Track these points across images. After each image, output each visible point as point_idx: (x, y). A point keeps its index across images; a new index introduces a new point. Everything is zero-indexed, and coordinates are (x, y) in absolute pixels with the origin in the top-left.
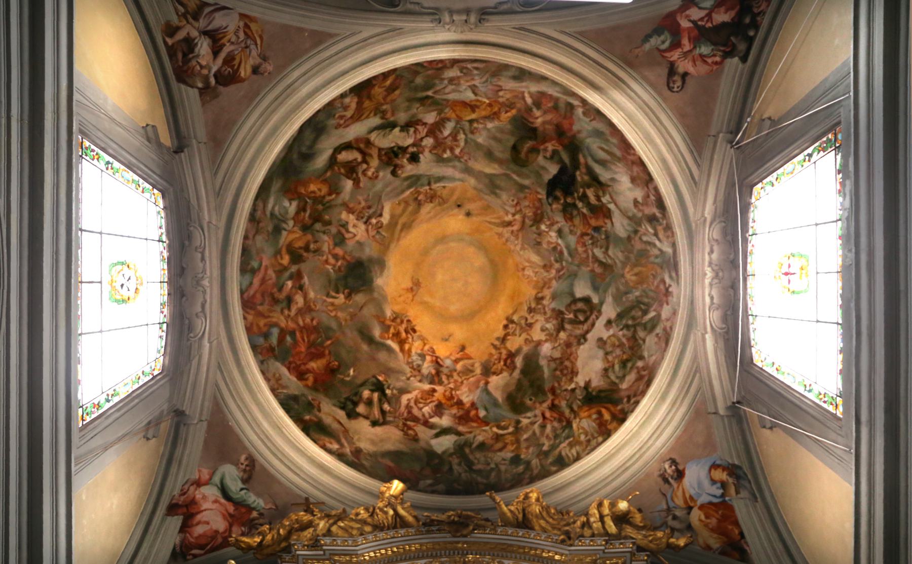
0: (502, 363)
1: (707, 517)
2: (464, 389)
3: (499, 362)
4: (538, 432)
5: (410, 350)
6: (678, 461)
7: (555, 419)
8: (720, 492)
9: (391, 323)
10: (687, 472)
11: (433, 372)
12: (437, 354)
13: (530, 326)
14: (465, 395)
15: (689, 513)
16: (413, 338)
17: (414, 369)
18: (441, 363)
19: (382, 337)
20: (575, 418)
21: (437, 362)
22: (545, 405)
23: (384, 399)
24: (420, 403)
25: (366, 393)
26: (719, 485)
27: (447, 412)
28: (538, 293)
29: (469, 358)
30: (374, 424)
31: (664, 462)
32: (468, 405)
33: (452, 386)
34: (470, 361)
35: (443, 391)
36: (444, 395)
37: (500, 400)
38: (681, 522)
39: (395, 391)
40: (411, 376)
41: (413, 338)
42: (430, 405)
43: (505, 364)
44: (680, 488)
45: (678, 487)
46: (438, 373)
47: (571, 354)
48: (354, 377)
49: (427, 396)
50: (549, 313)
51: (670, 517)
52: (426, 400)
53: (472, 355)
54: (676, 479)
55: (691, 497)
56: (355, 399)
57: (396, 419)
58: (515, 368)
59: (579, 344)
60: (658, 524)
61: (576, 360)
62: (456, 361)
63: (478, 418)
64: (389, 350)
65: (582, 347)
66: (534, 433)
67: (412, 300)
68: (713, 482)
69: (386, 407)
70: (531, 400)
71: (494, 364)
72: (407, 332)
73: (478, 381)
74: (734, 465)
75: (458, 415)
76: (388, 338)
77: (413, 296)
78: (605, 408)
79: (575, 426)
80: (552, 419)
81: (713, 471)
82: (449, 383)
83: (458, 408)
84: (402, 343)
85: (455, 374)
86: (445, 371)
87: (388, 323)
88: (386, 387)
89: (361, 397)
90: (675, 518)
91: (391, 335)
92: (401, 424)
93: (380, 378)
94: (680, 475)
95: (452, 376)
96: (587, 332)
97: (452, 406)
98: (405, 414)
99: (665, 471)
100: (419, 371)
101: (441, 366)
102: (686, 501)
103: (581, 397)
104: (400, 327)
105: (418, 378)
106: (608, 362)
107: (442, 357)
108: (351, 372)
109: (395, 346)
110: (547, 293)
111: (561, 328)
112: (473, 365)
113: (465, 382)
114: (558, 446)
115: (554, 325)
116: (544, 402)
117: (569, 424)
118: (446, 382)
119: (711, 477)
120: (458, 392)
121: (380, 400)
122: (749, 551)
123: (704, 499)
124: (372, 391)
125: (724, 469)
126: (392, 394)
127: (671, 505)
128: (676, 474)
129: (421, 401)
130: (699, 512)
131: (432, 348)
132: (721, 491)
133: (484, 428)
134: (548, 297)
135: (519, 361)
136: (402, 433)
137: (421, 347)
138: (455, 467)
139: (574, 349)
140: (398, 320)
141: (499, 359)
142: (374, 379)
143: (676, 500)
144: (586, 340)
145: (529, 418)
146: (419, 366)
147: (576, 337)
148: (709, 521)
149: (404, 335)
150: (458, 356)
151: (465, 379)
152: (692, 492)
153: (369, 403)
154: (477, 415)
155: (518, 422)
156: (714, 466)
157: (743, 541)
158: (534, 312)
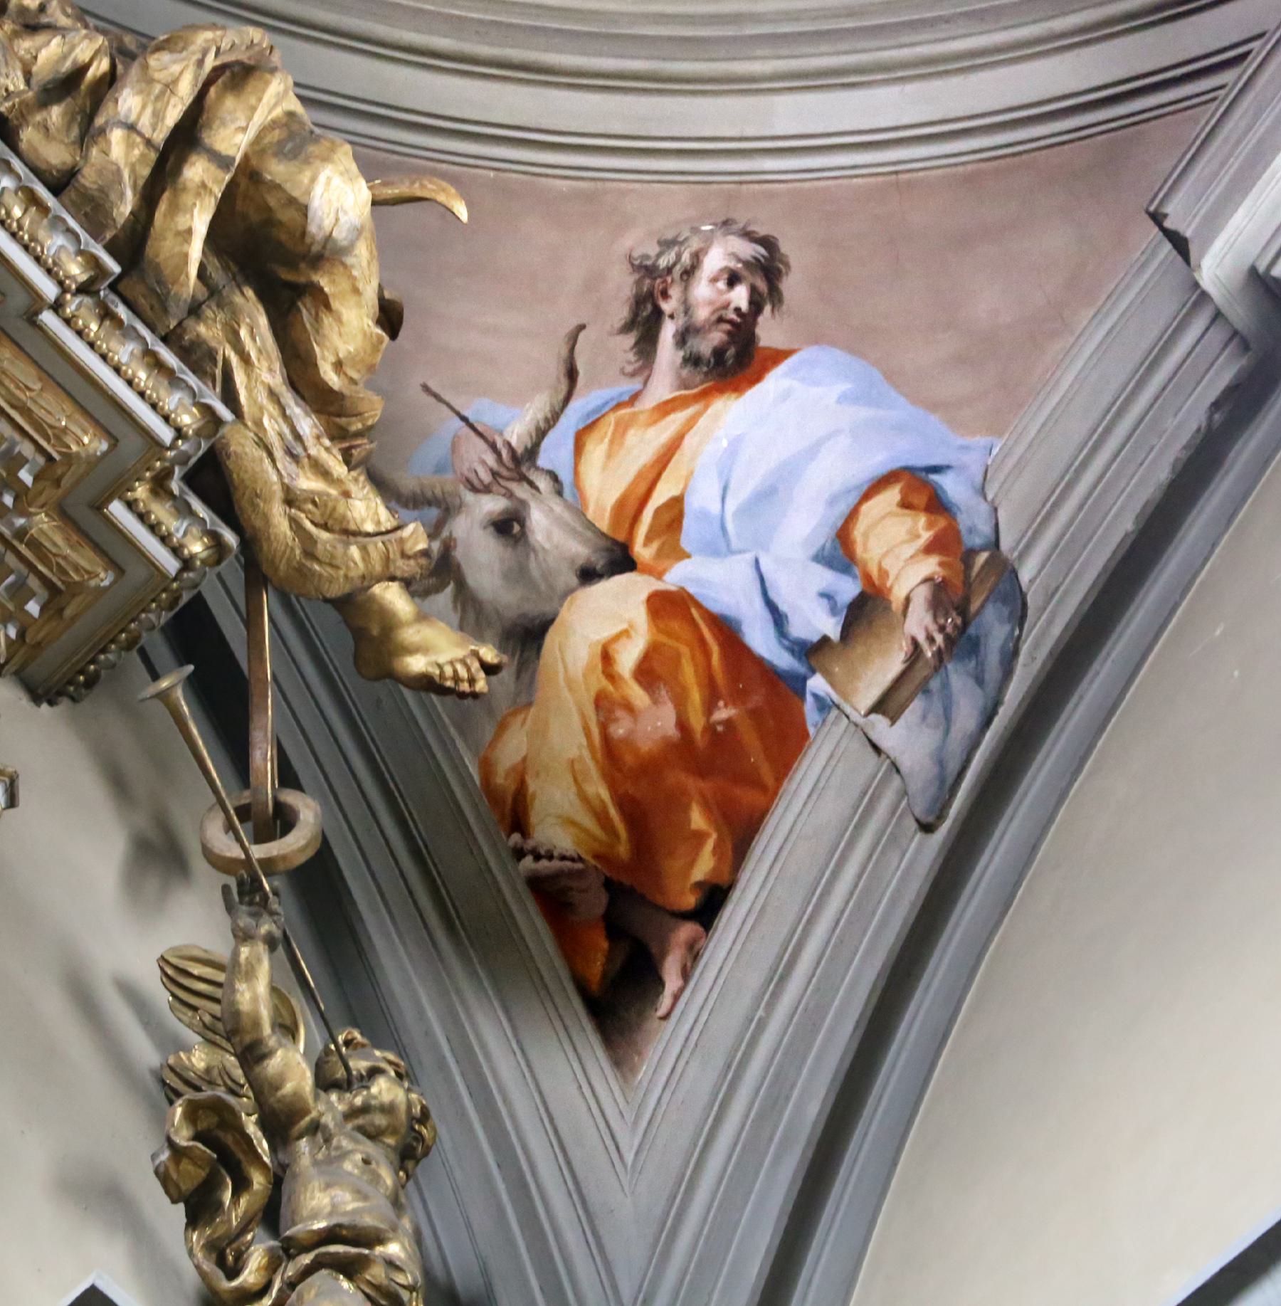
1: (647, 673)
6: (789, 285)
10: (775, 381)
15: (588, 575)
26: (848, 589)
31: (726, 224)
38: (518, 574)
44: (677, 419)
45: (666, 408)
51: (492, 505)
54: (693, 360)
55: (674, 514)
60: (408, 481)
74: (1004, 570)
81: (892, 495)
99: (689, 273)
102: (631, 508)
119: (853, 515)
122: (665, 1001)
127: (555, 453)
128: (717, 337)
130: (639, 615)
143: (596, 451)
148: (638, 695)
157: (687, 931)
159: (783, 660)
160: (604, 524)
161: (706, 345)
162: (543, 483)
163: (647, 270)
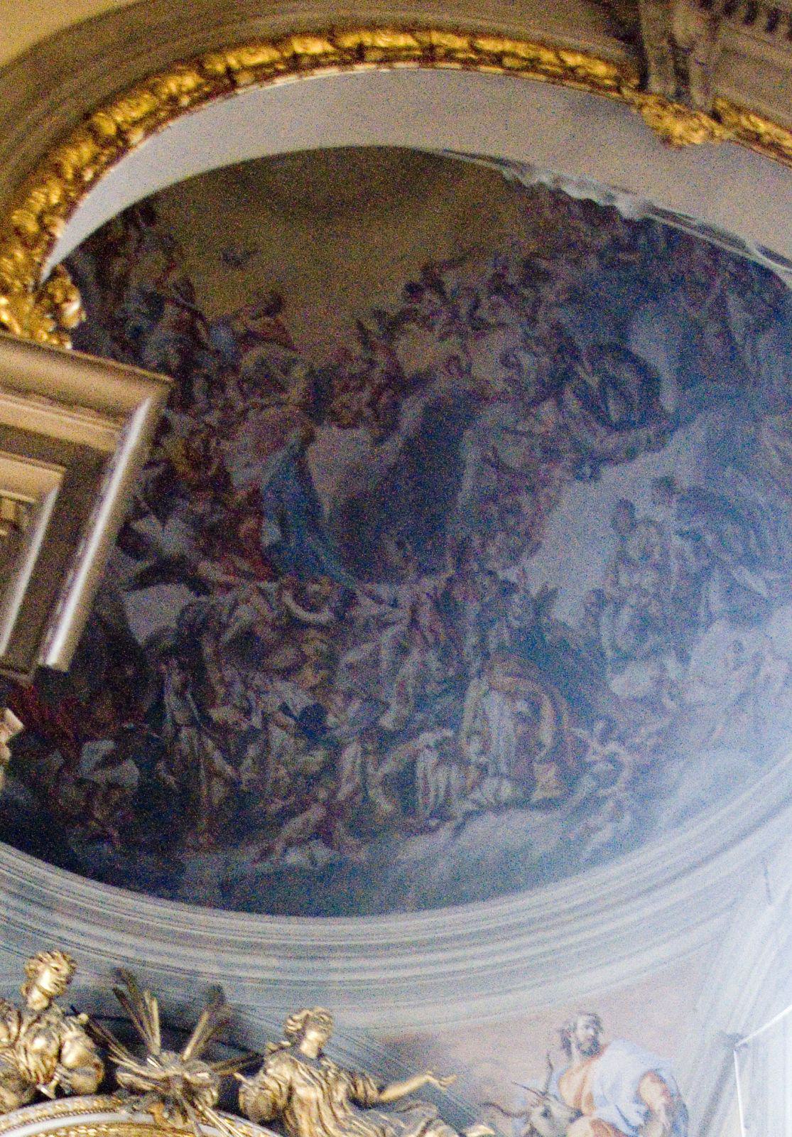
0: (366, 395)
2: (245, 436)
3: (360, 388)
4: (386, 655)
7: (437, 642)
8: (637, 1120)
10: (607, 1053)
13: (480, 328)
14: (243, 459)
15: (572, 1121)
20: (480, 674)
21: (193, 332)
22: (429, 583)
26: (643, 1109)
29: (288, 345)
31: (581, 1013)
32: (241, 496)
33: (213, 418)
34: (284, 354)
37: (327, 509)
38: (553, 1127)
43: (372, 404)
44: (583, 1071)
47: (545, 483)
50: (543, 328)
51: (541, 1109)
55: (590, 1100)
58: (393, 427)
62: (248, 339)
63: (258, 543)
65: (577, 484)
68: (638, 1099)
70: (400, 545)
71: (346, 388)
73: (286, 424)
78: (554, 704)
79: (472, 693)
80: (431, 638)
81: (648, 1080)
82: (211, 408)
83: (216, 500)
85: (231, 382)
86: (210, 365)
90: (546, 1114)
94: (594, 1050)
96: (609, 459)
97: (199, 488)
99: (575, 1029)
101: (201, 345)
102: (578, 1098)
106: (616, 583)
112: (286, 372)
113: (251, 414)
114: (413, 735)
116: (432, 571)
117: (458, 685)
120: (226, 445)
123: (607, 1113)
125: (665, 1092)
127: (553, 1090)
132: (637, 1120)
135: (411, 412)
141: (363, 378)
143: (564, 1085)
144: (595, 476)
145: (379, 601)
150: (256, 326)
152: (597, 1091)
155: (349, 600)
156: (655, 1075)
158: (506, 298)
159: (630, 1132)
160: (572, 1105)
161: (586, 1047)
162: (552, 1099)
163: (562, 1031)
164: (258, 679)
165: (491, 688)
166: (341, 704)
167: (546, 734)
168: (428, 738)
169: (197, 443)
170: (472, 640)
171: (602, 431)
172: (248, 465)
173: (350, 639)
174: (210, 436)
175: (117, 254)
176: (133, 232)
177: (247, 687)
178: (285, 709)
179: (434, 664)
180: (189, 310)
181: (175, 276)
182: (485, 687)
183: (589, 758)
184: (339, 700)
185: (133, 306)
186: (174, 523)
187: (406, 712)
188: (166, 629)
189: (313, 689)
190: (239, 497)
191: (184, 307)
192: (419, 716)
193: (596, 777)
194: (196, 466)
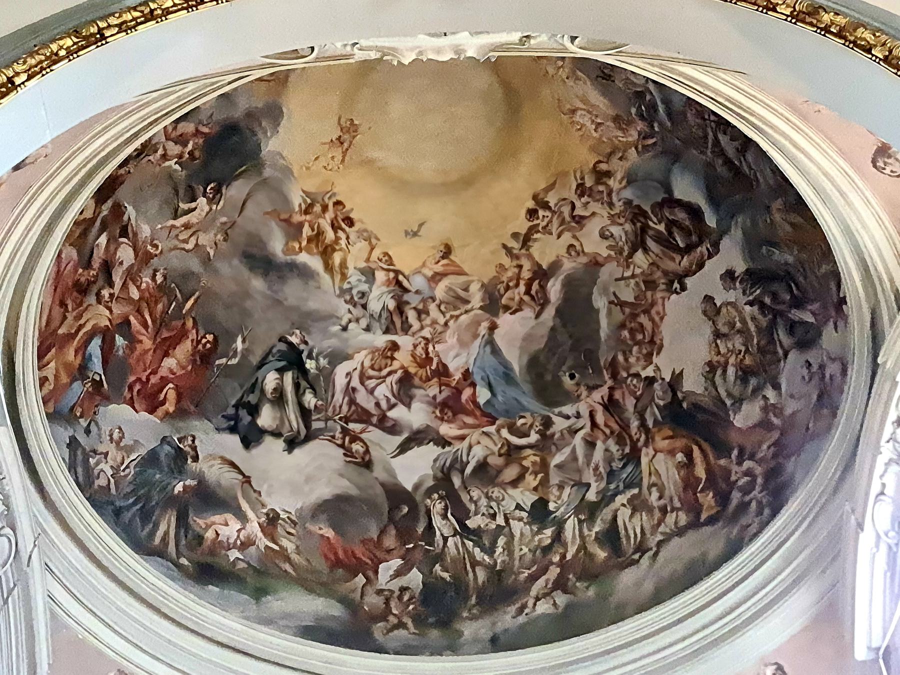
2: (451, 338)
5: (343, 265)
9: (303, 218)
11: (392, 305)
12: (398, 266)
14: (452, 354)
16: (348, 238)
17: (355, 306)
18: (405, 283)
19: (287, 250)
20: (646, 444)
21: (399, 283)
23: (303, 384)
24: (370, 378)
25: (271, 380)
27: (418, 392)
28: (600, 162)
30: (292, 444)
33: (426, 333)
35: (411, 348)
36: (413, 356)
39: (323, 362)
40: (350, 321)
41: (348, 238)
42: (389, 380)
46: (400, 308)
48: (246, 352)
49: (383, 362)
52: (380, 370)
53: (466, 270)
56: (252, 398)
57: (330, 423)
59: (670, 290)
61: (662, 319)
64: (305, 273)
65: (674, 296)
66: (574, 457)
67: (343, 161)
69: (310, 400)
72: (335, 227)
75: (439, 399)
76: (301, 249)
77: (344, 153)
79: (644, 460)
82: (422, 328)
84: (326, 253)
85: (432, 307)
86: (414, 300)
87: (297, 218)
88: (304, 356)
89: (262, 391)
91: (304, 243)
92: (338, 435)
93: (294, 340)
95: (428, 313)
98: (345, 408)
100: (364, 307)
101: (406, 291)
103: (661, 403)
104: (321, 221)
105: (364, 323)
107: (407, 274)
108: (239, 344)
109: (315, 262)
110: (619, 168)
111: (638, 243)
114: (612, 498)
115: (626, 233)
117: (633, 457)
118: (416, 325)
121: (297, 386)
124: (281, 371)
126: (317, 368)
129: (371, 373)
131: (386, 254)
133: (485, 429)
134: (619, 176)
136: (342, 451)
137: (366, 256)
138: (437, 521)
139: (659, 295)
140: (318, 208)
142: (283, 347)
144: (683, 288)
146: (363, 295)
147: (666, 273)
149: (330, 235)
151: (452, 317)
153: (279, 399)
154: (473, 399)
164: (496, 492)
165: (656, 451)
166: (558, 494)
167: (700, 471)
168: (621, 499)
169: (420, 351)
170: (635, 424)
171: (678, 258)
172: (457, 356)
173: (553, 448)
174: (426, 344)
175: (334, 250)
176: (341, 234)
177: (489, 498)
178: (519, 507)
179: (614, 448)
180: (394, 271)
181: (377, 253)
182: (652, 452)
183: (733, 478)
184: (555, 491)
185: (354, 277)
186: (416, 405)
187: (603, 485)
188: (426, 475)
189: (535, 489)
190: (457, 378)
191: (388, 270)
192: (612, 486)
193: (741, 489)
194: (421, 366)
